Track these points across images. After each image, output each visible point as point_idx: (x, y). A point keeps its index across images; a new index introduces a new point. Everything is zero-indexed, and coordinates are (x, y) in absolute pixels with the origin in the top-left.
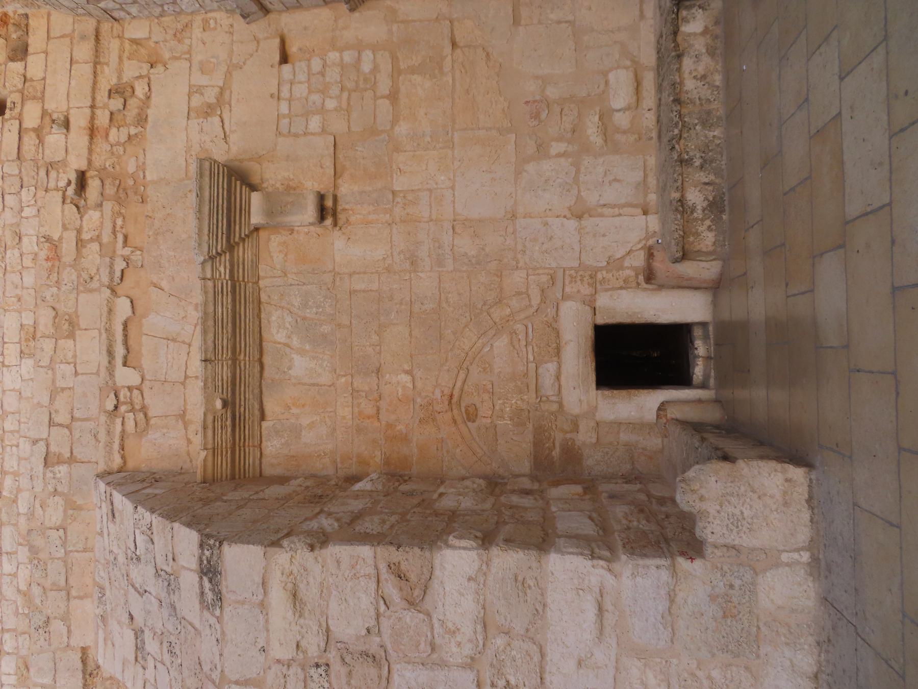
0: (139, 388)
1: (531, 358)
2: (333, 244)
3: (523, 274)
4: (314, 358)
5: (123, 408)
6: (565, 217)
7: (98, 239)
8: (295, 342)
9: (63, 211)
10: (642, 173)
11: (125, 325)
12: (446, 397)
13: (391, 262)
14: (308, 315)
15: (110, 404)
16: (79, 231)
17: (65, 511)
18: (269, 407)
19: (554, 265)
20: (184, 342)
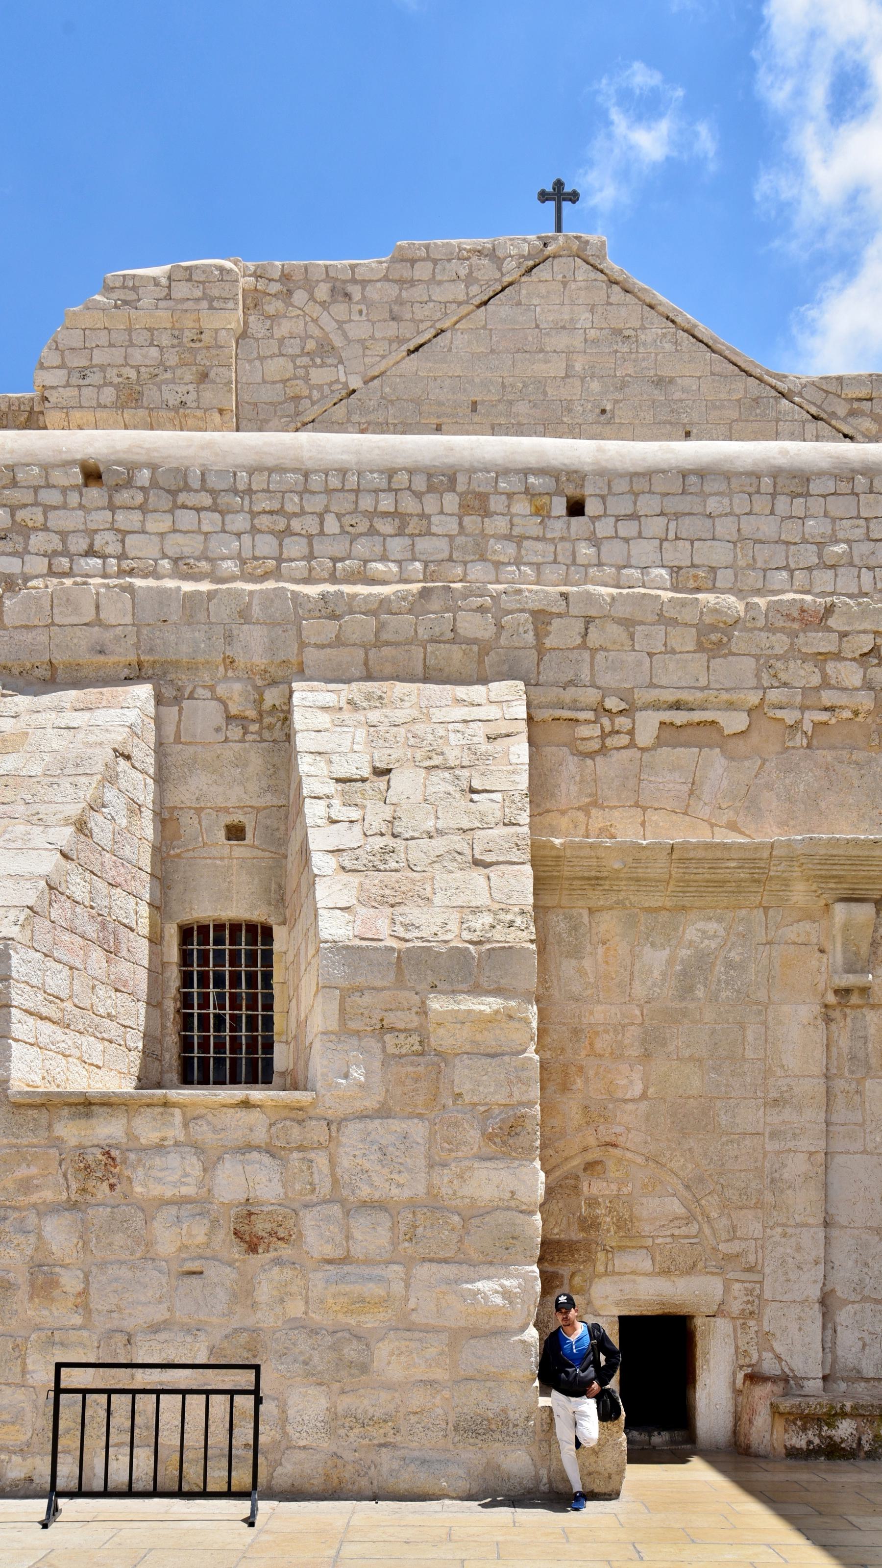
0: (632, 744)
1: (659, 1241)
2: (804, 1002)
3: (758, 1234)
4: (664, 975)
5: (606, 721)
6: (824, 1284)
7: (826, 684)
8: (684, 953)
9: (864, 632)
10: (872, 1375)
11: (713, 722)
12: (614, 1139)
13: (778, 1074)
14: (717, 968)
15: (612, 703)
16: (837, 656)
17: (474, 641)
18: (606, 916)
19: (767, 1270)
20: (688, 806)
